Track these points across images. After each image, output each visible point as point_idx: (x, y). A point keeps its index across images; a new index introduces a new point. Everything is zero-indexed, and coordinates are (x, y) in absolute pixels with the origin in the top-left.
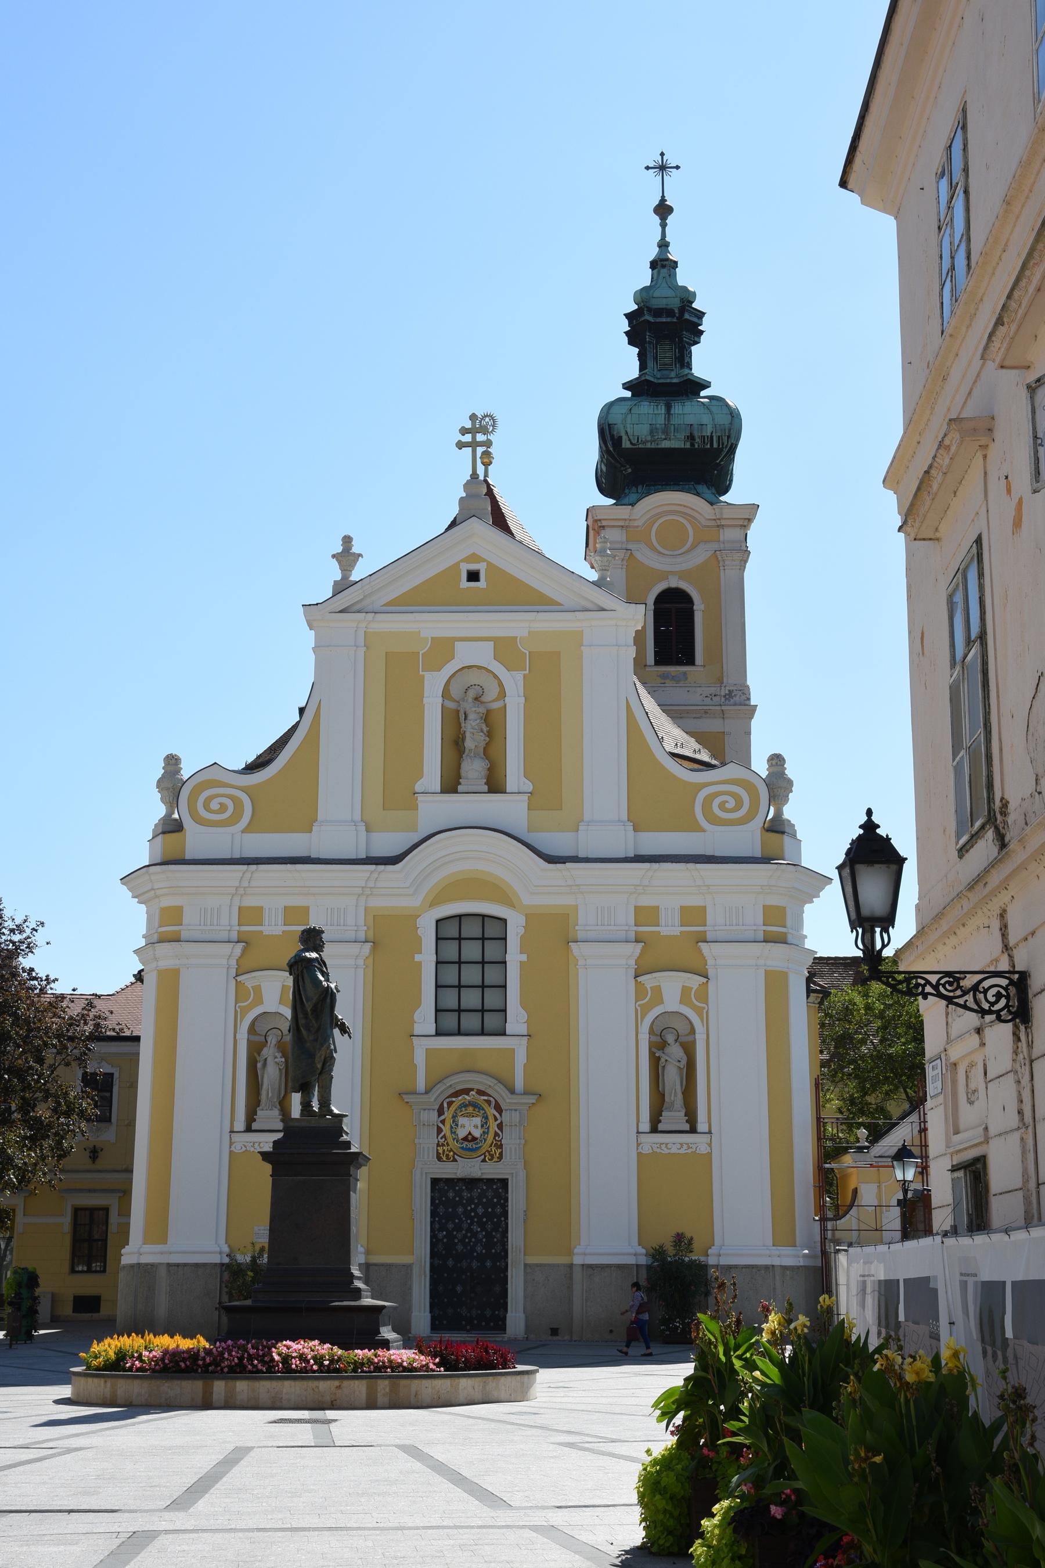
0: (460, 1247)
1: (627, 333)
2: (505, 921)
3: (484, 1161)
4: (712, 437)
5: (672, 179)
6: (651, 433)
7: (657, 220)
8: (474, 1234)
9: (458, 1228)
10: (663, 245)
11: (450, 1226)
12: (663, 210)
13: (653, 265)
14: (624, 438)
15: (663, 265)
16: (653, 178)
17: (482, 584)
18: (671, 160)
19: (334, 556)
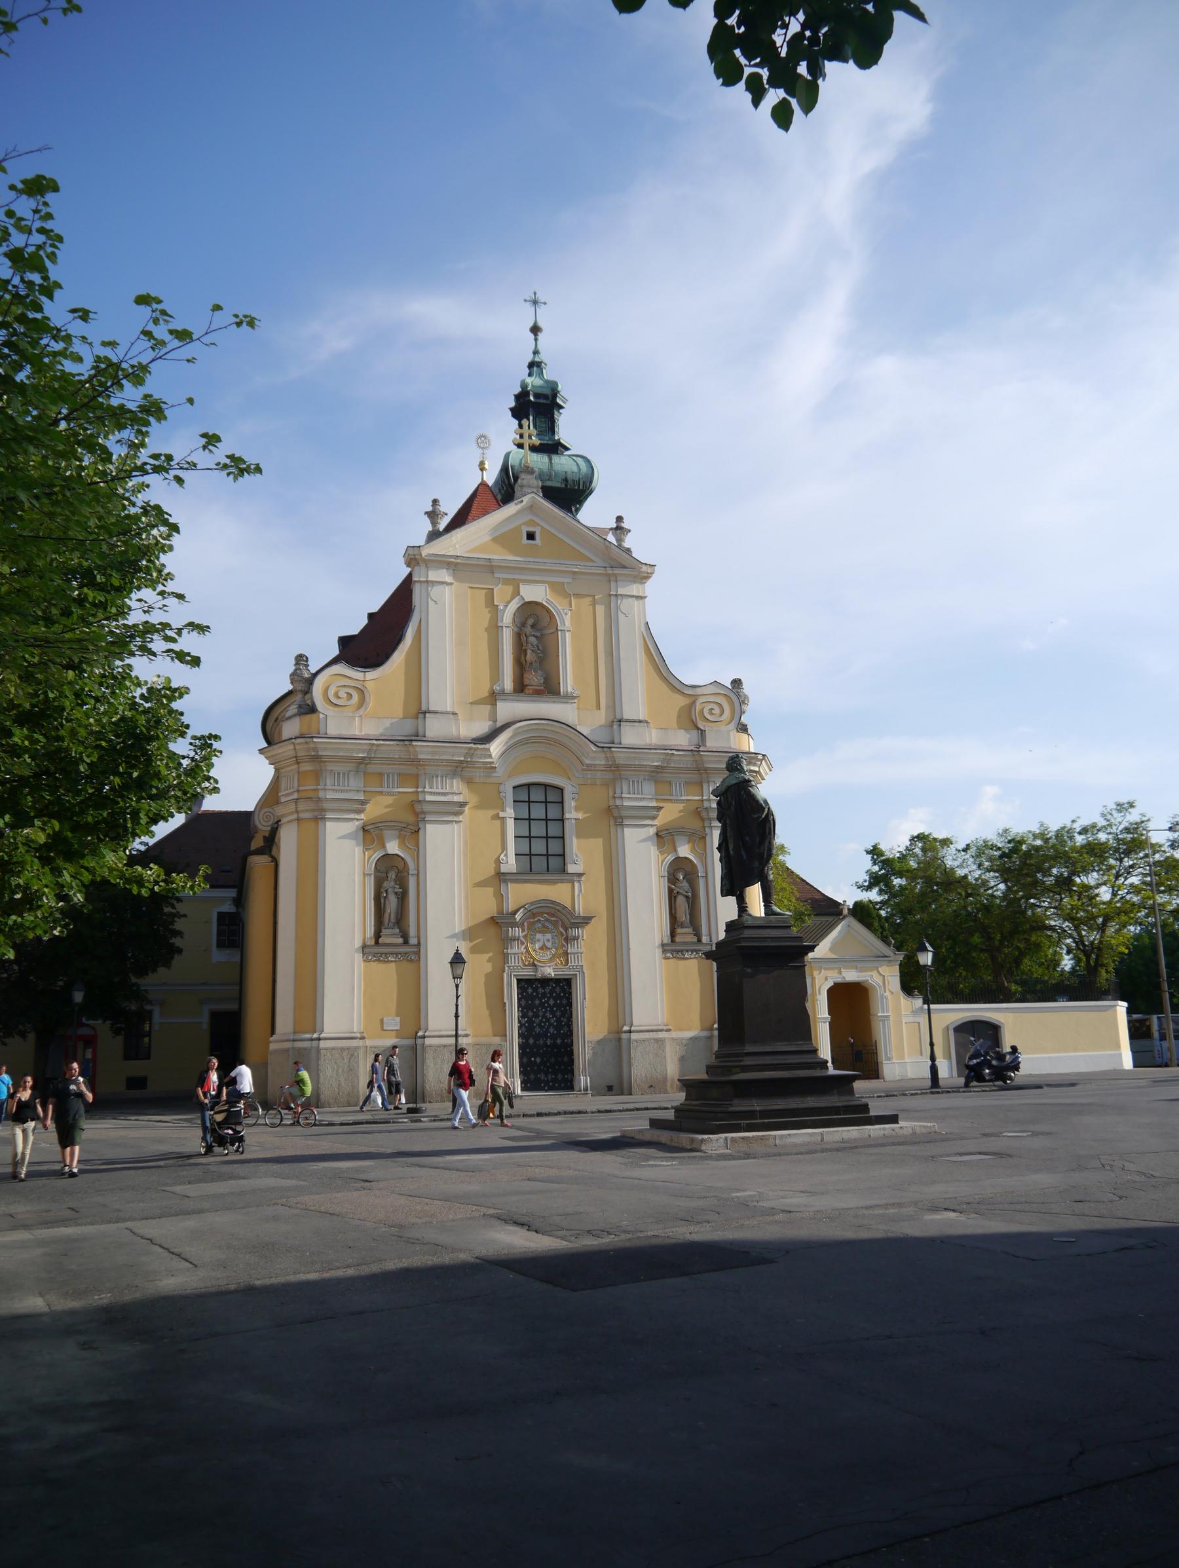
0: (538, 1030)
1: (512, 410)
2: (561, 790)
5: (541, 310)
7: (532, 336)
8: (548, 1020)
9: (537, 1016)
11: (530, 1014)
12: (535, 330)
16: (530, 308)
17: (538, 541)
18: (541, 297)
19: (426, 513)
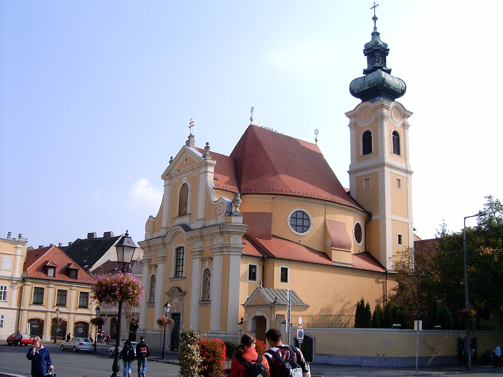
3: (177, 309)
7: (373, 21)
10: (375, 28)
12: (375, 19)
13: (373, 34)
14: (354, 90)
15: (375, 34)
16: (373, 10)
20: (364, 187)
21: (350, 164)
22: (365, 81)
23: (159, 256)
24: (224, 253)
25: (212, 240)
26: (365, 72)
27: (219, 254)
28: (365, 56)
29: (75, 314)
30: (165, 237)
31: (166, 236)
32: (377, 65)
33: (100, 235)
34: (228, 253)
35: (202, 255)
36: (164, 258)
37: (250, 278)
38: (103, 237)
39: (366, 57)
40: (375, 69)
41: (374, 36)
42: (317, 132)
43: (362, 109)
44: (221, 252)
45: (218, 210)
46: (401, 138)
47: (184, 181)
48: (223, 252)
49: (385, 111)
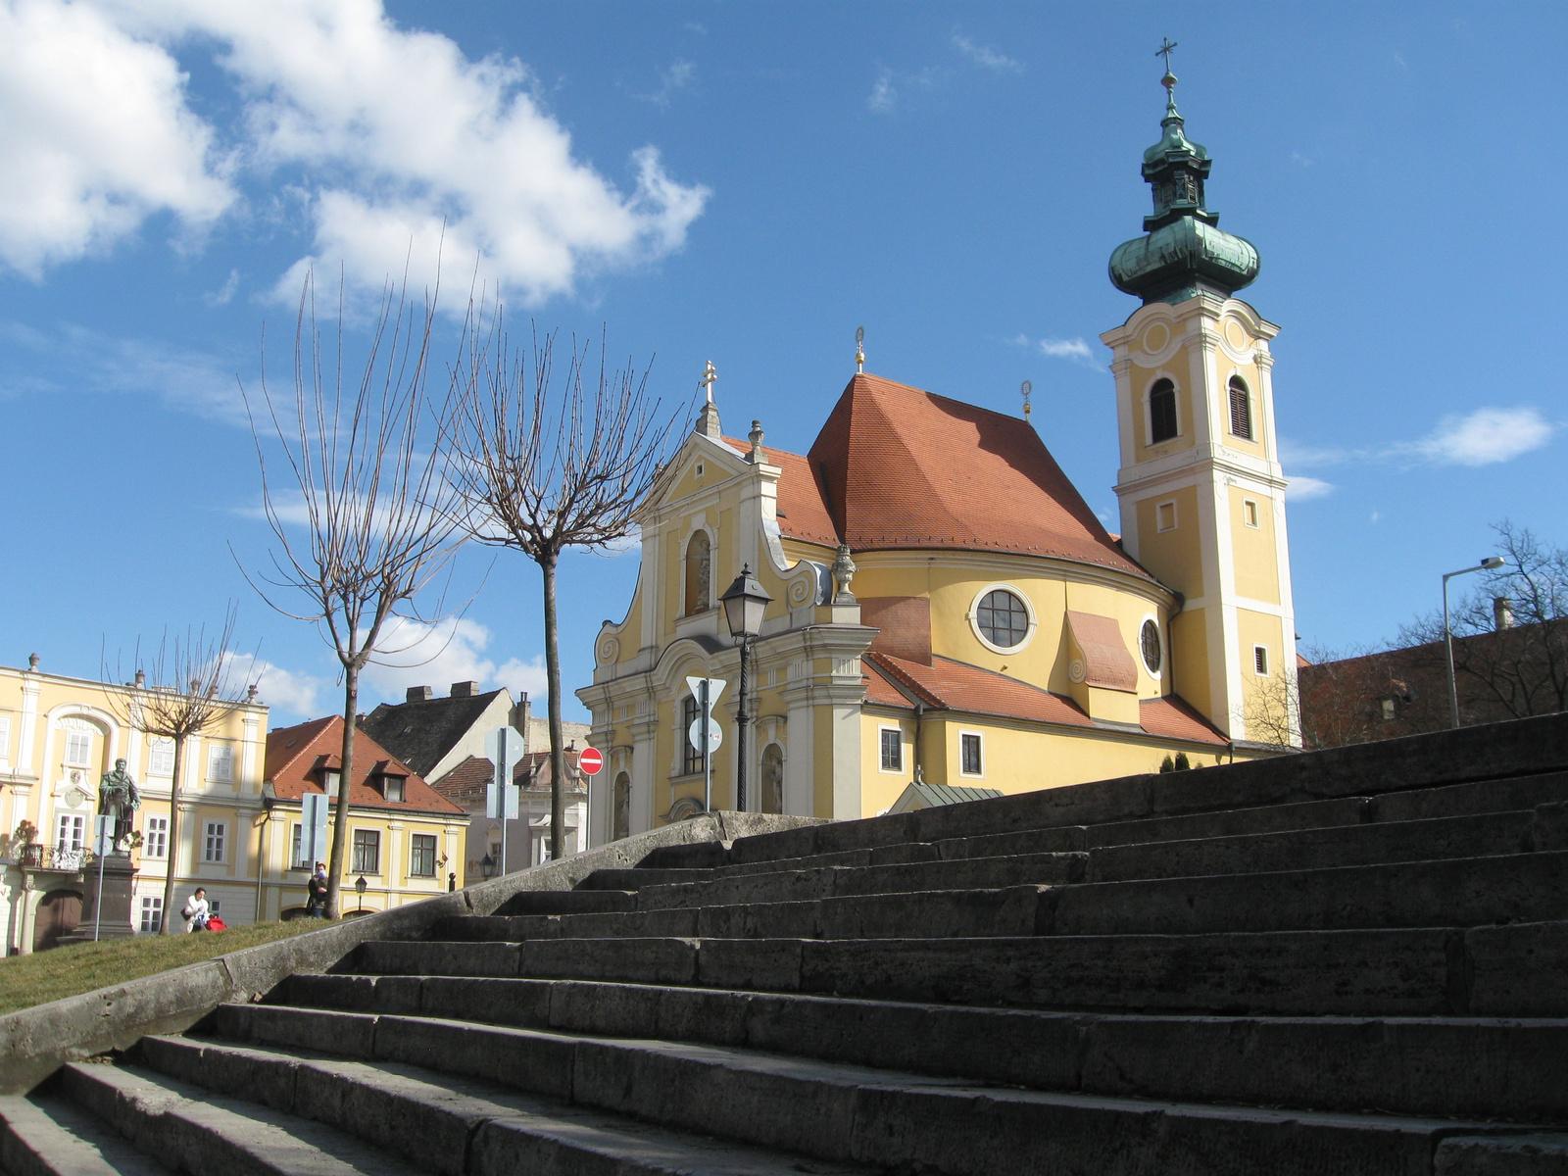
4: (1175, 250)
6: (1138, 264)
12: (1168, 82)
20: (1160, 526)
21: (1119, 467)
22: (1151, 248)
23: (637, 721)
24: (817, 702)
25: (783, 669)
26: (1151, 225)
27: (805, 703)
28: (1146, 181)
29: (401, 892)
30: (655, 672)
31: (655, 669)
32: (1181, 203)
33: (440, 689)
34: (827, 701)
35: (757, 710)
36: (652, 726)
37: (886, 764)
38: (449, 695)
39: (1149, 185)
40: (1177, 215)
41: (1167, 129)
42: (1026, 389)
43: (1146, 321)
44: (807, 699)
45: (794, 593)
46: (1252, 395)
47: (698, 523)
48: (813, 698)
49: (1207, 324)
